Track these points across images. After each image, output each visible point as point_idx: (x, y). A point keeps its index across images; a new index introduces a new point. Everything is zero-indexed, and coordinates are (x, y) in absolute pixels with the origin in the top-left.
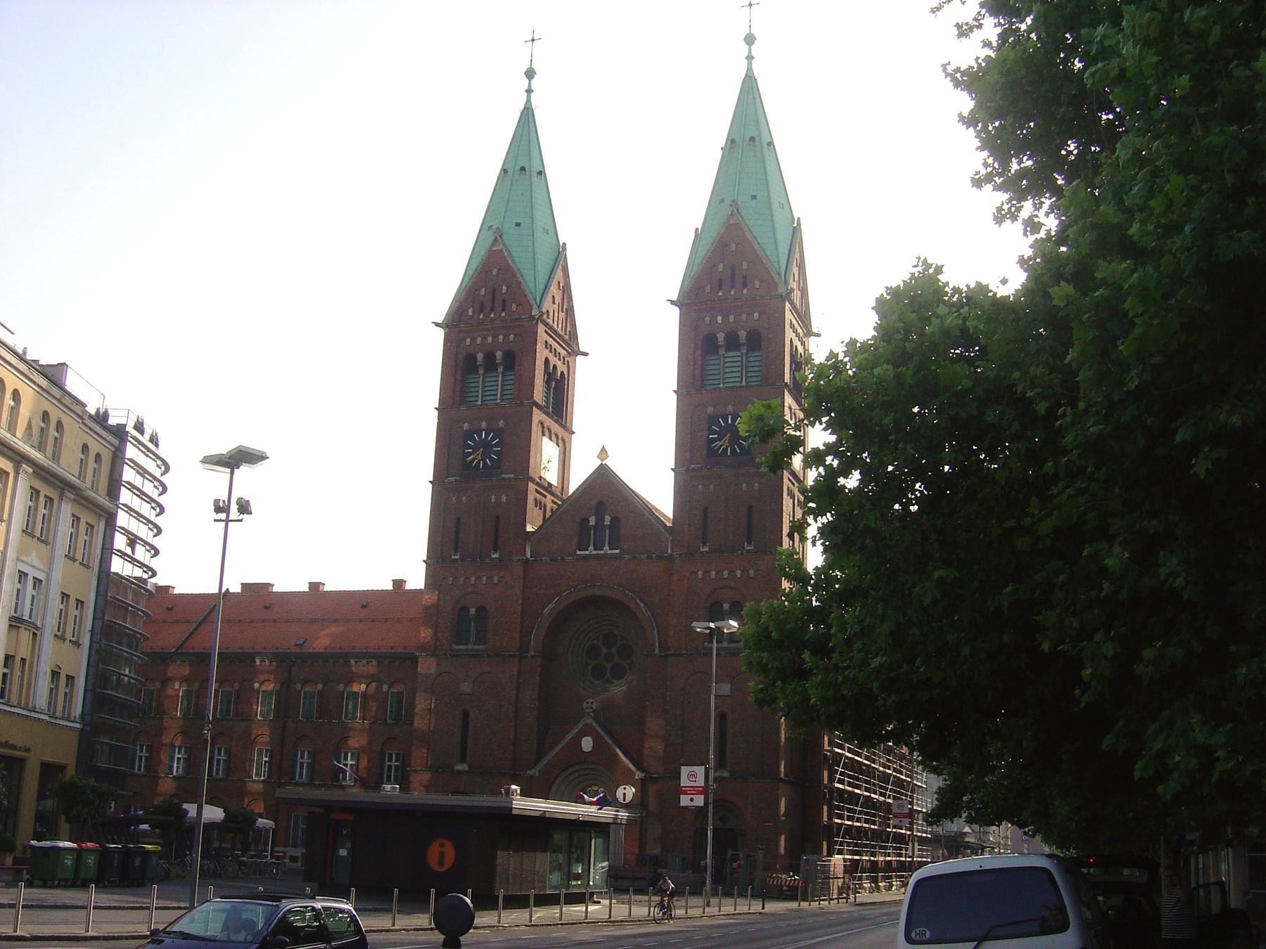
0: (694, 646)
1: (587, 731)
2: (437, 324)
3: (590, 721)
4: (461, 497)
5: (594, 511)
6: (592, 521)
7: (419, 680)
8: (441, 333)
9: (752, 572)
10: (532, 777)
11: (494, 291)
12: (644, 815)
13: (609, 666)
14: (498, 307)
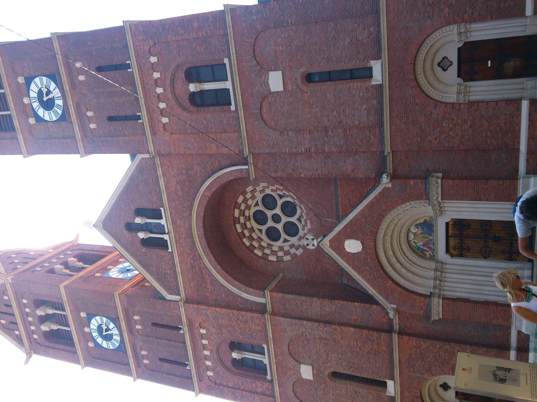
0: (235, 123)
2: (27, 361)
3: (326, 242)
5: (134, 234)
6: (142, 235)
9: (153, 59)
12: (440, 175)
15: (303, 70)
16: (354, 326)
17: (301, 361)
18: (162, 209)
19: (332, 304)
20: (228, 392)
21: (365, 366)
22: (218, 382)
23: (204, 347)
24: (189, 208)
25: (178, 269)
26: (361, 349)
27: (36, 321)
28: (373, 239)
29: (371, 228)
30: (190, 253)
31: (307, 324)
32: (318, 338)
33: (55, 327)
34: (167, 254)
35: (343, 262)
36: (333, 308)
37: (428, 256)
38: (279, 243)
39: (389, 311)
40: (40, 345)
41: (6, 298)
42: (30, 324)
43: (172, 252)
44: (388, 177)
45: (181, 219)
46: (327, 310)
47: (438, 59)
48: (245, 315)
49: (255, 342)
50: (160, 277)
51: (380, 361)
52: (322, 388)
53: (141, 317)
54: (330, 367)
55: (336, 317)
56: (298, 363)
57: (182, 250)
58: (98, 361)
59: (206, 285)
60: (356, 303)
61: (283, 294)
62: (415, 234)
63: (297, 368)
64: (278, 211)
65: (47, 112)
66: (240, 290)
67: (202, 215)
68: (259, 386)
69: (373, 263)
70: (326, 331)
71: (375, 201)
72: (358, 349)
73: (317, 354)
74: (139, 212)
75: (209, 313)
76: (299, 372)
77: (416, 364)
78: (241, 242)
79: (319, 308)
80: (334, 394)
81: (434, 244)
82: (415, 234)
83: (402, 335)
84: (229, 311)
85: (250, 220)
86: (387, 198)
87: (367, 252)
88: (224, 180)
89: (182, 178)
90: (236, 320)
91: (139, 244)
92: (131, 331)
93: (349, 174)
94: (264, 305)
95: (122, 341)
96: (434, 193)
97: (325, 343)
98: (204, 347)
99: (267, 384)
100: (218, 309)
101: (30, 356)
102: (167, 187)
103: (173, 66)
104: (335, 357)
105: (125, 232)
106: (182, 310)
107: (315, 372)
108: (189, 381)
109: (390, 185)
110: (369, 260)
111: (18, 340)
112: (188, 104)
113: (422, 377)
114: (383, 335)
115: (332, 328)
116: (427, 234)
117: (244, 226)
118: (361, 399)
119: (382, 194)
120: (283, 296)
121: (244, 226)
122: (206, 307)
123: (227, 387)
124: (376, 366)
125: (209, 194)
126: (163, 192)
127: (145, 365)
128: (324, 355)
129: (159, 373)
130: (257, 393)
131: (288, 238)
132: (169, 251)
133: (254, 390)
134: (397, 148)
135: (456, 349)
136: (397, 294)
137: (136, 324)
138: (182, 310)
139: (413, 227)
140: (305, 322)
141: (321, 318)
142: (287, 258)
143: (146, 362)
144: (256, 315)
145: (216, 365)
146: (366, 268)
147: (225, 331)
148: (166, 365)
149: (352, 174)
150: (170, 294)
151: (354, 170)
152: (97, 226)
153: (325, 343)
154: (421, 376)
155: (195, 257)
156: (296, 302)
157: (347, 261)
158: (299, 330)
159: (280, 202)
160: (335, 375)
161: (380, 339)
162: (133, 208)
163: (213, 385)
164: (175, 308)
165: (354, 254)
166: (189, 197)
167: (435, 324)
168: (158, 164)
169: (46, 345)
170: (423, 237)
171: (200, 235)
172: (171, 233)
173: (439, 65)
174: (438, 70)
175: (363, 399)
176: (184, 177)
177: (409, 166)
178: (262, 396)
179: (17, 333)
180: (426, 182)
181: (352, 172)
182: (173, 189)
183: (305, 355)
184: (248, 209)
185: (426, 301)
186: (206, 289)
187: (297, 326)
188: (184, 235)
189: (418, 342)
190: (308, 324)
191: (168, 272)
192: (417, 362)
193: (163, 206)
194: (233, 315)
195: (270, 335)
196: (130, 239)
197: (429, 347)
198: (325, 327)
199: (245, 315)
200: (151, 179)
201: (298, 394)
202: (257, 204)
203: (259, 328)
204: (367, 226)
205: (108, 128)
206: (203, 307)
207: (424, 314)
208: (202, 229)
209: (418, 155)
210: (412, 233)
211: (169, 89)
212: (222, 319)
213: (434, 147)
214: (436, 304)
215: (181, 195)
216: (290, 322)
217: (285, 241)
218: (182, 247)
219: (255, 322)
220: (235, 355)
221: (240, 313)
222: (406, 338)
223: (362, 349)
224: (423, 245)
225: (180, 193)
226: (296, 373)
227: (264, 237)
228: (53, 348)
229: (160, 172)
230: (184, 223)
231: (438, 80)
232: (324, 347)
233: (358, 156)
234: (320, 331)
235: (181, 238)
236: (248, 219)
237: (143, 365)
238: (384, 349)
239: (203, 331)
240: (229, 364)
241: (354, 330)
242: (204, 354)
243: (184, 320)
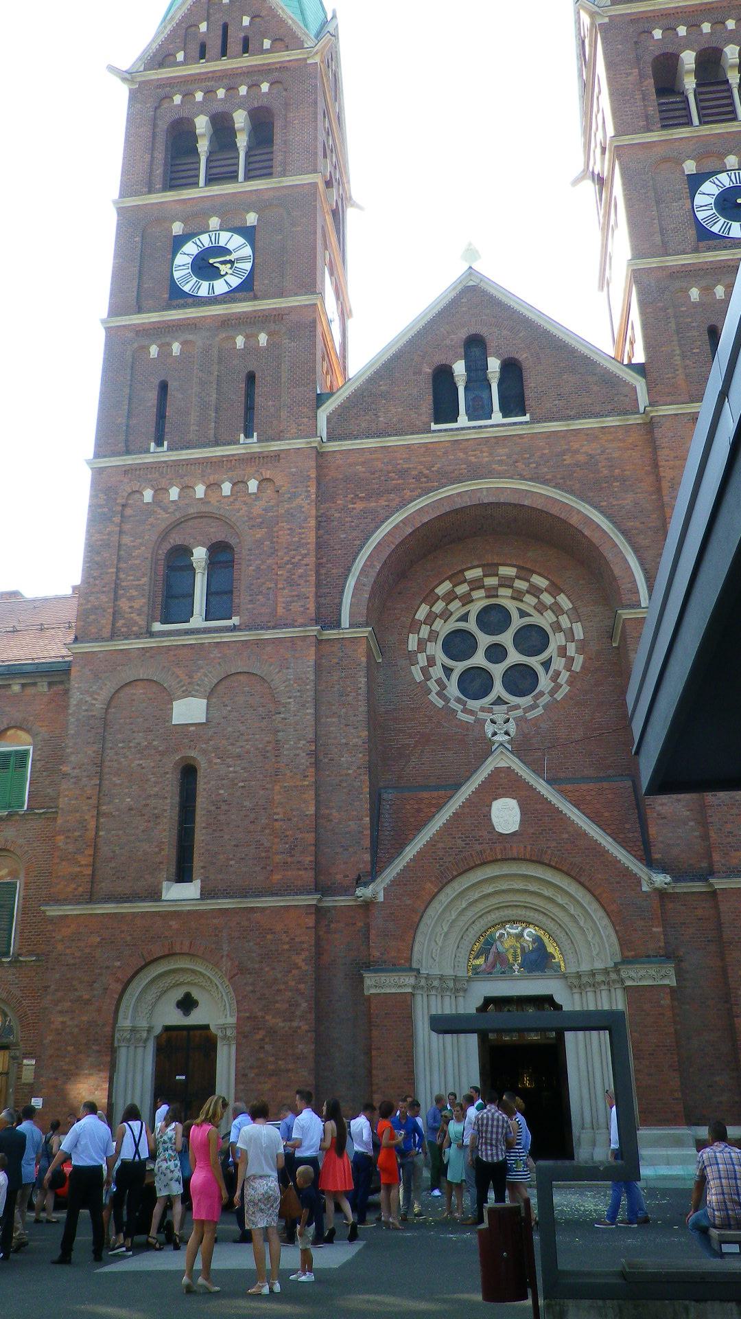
1: (503, 784)
2: (112, 69)
3: (502, 760)
4: (170, 345)
6: (459, 368)
7: (73, 702)
8: (121, 93)
10: (368, 905)
11: (225, 27)
13: (497, 670)
14: (234, 45)
16: (317, 816)
17: (214, 700)
18: (527, 418)
19: (359, 768)
20: (108, 534)
21: (227, 837)
22: (128, 512)
23: (213, 486)
24: (536, 475)
25: (392, 441)
26: (265, 828)
27: (218, 108)
28: (525, 854)
29: (549, 852)
30: (433, 469)
31: (308, 714)
32: (279, 738)
33: (203, 146)
34: (425, 418)
35: (466, 796)
36: (350, 772)
37: (478, 962)
38: (441, 658)
39: (371, 887)
40: (156, 108)
41: (267, 44)
42: (209, 92)
43: (429, 431)
44: (666, 884)
45: (509, 456)
46: (342, 759)
48: (308, 581)
49: (242, 598)
50: (365, 399)
51: (244, 869)
52: (155, 743)
53: (267, 349)
54: (210, 762)
55: (329, 776)
56: (210, 693)
57: (438, 453)
58: (137, 239)
60: (368, 819)
61: (364, 664)
62: (520, 936)
63: (197, 691)
64: (514, 657)
65: (712, 201)
66: (360, 573)
67: (526, 503)
68: (135, 604)
69: (471, 855)
70: (298, 755)
71: (610, 859)
72: (264, 821)
73: (237, 734)
74: (511, 369)
75: (298, 501)
76: (187, 694)
77: (251, 944)
78: (445, 576)
79: (344, 741)
80: (143, 768)
81: (503, 973)
82: (520, 936)
83: (315, 914)
84: (312, 547)
85: (488, 597)
86: (618, 883)
87: (496, 843)
88: (610, 555)
89: (603, 467)
90: (293, 560)
91: (440, 359)
92: (228, 324)
93: (654, 808)
94: (338, 625)
95: (199, 302)
96: (642, 972)
97: (267, 752)
98: (213, 486)
99: (143, 623)
100: (313, 523)
101: (124, 80)
102: (579, 433)
104: (235, 772)
105: (463, 334)
106: (299, 443)
107: (192, 728)
108: (121, 446)
109: (645, 888)
110: (478, 848)
111: (160, 57)
113: (222, 957)
114: (308, 876)
115: (307, 767)
116: (524, 960)
117: (477, 584)
118: (142, 828)
119: (626, 873)
120: (359, 665)
121: (476, 584)
122: (313, 496)
123: (121, 532)
124: (231, 859)
125: (574, 520)
126: (568, 425)
127: (145, 349)
128: (237, 750)
129: (129, 378)
130: (116, 599)
131: (455, 676)
132: (432, 424)
133: (122, 592)
134: (723, 901)
135: (301, 1024)
136: (409, 902)
137: (247, 337)
138: (299, 443)
139: (534, 932)
140: (311, 711)
141: (321, 745)
142: (419, 677)
143: (154, 351)
144: (312, 606)
145: (169, 511)
146: (459, 841)
147: (260, 534)
148: (152, 396)
149: (655, 815)
150: (329, 420)
151: (662, 818)
152: (470, 274)
153: (267, 752)
154: (225, 953)
155: (425, 479)
156: (350, 692)
157: (469, 802)
158: (290, 698)
159: (534, 662)
160: (189, 773)
161: (299, 869)
162: (522, 356)
164: (300, 428)
165: (488, 816)
166: (561, 479)
167: (346, 979)
168: (628, 419)
169: (159, 123)
170: (515, 952)
171: (479, 495)
172: (476, 433)
175: (143, 831)
176: (606, 472)
177: (685, 923)
178: (111, 610)
179: (180, 56)
180: (661, 956)
181: (658, 815)
182: (576, 446)
183: (229, 708)
184: (515, 595)
185: (403, 961)
186: (352, 498)
187: (299, 694)
188: (473, 459)
189: (305, 946)
190: (308, 717)
191: (380, 419)
192: (256, 944)
193: (533, 421)
194: (305, 556)
195: (268, 635)
196: (448, 342)
197: (298, 968)
198: (308, 754)
199: (308, 581)
200: (590, 402)
201: (127, 689)
202: (523, 614)
203: (280, 611)
204: (554, 844)
205: (694, 324)
206: (313, 490)
207: (371, 956)
208: (492, 499)
209: (708, 941)
210: (523, 930)
212: (289, 529)
213: (732, 969)
214: (402, 980)
215: (565, 462)
216: (308, 678)
217: (448, 671)
218: (446, 453)
219: (293, 602)
220: (200, 554)
221: (311, 571)
222: (311, 921)
223: (267, 831)
224: (498, 953)
225: (568, 459)
226: (184, 688)
227: (452, 625)
228: (154, 136)
229: (611, 421)
230: (501, 462)
232: (257, 749)
233: (692, 826)
234: (295, 743)
235: (466, 453)
236: (492, 593)
238: (277, 877)
239: (253, 485)
240: (176, 539)
241: (311, 815)
242: (196, 484)
243: (275, 446)
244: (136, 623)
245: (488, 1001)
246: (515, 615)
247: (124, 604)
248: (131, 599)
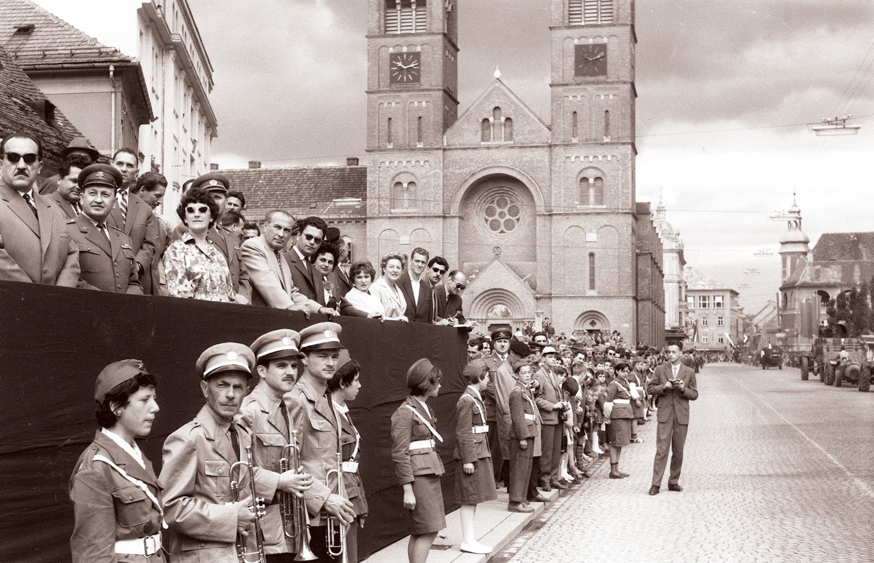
13: (502, 221)
15: (597, 254)
22: (381, 169)
47: (596, 321)
59: (458, 169)
64: (508, 217)
84: (441, 187)
103: (605, 171)
112: (582, 176)
137: (419, 102)
163: (378, 165)
173: (593, 321)
174: (590, 321)
194: (439, 190)
203: (432, 209)
211: (591, 165)
225: (525, 159)
231: (586, 320)
237: (382, 102)
240: (397, 180)
244: (386, 210)
245: (491, 325)
246: (509, 202)
247: (382, 203)
248: (384, 201)
